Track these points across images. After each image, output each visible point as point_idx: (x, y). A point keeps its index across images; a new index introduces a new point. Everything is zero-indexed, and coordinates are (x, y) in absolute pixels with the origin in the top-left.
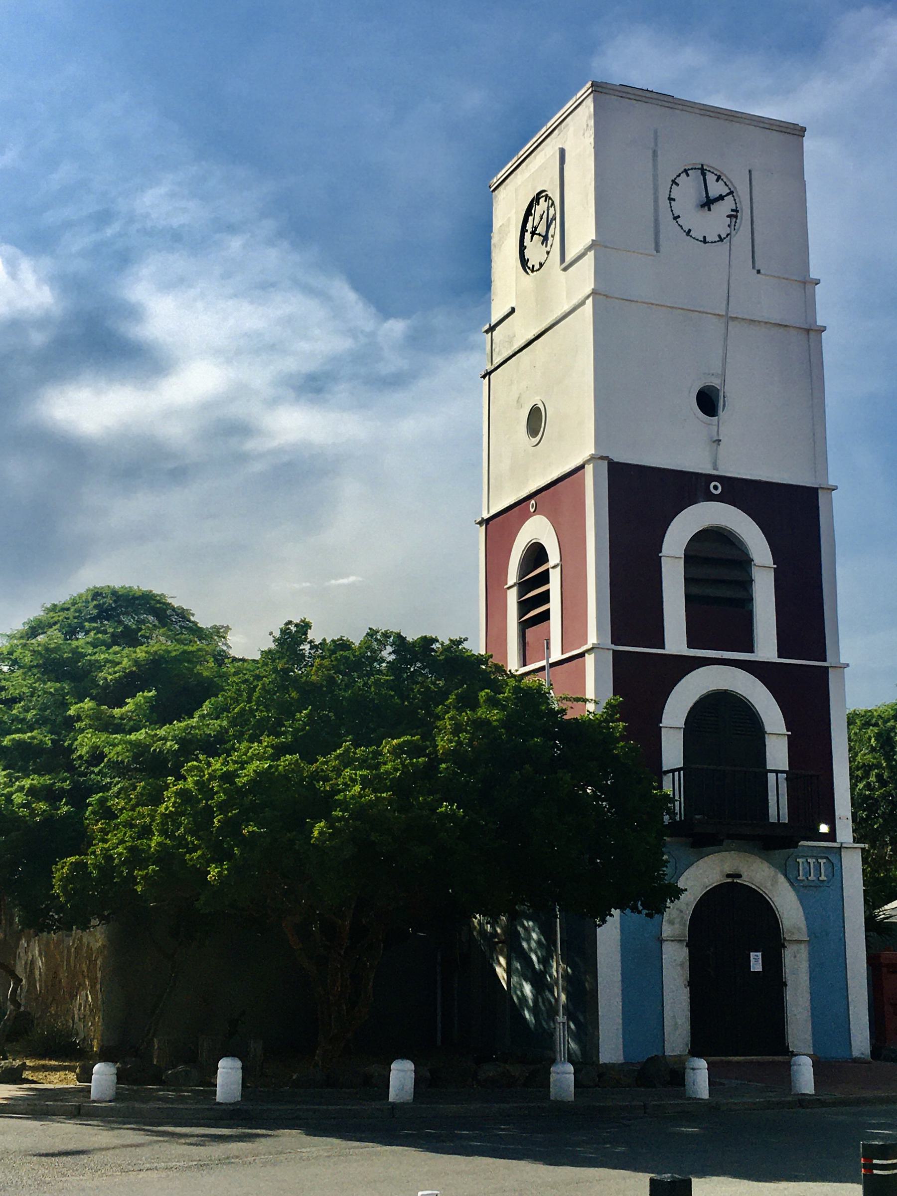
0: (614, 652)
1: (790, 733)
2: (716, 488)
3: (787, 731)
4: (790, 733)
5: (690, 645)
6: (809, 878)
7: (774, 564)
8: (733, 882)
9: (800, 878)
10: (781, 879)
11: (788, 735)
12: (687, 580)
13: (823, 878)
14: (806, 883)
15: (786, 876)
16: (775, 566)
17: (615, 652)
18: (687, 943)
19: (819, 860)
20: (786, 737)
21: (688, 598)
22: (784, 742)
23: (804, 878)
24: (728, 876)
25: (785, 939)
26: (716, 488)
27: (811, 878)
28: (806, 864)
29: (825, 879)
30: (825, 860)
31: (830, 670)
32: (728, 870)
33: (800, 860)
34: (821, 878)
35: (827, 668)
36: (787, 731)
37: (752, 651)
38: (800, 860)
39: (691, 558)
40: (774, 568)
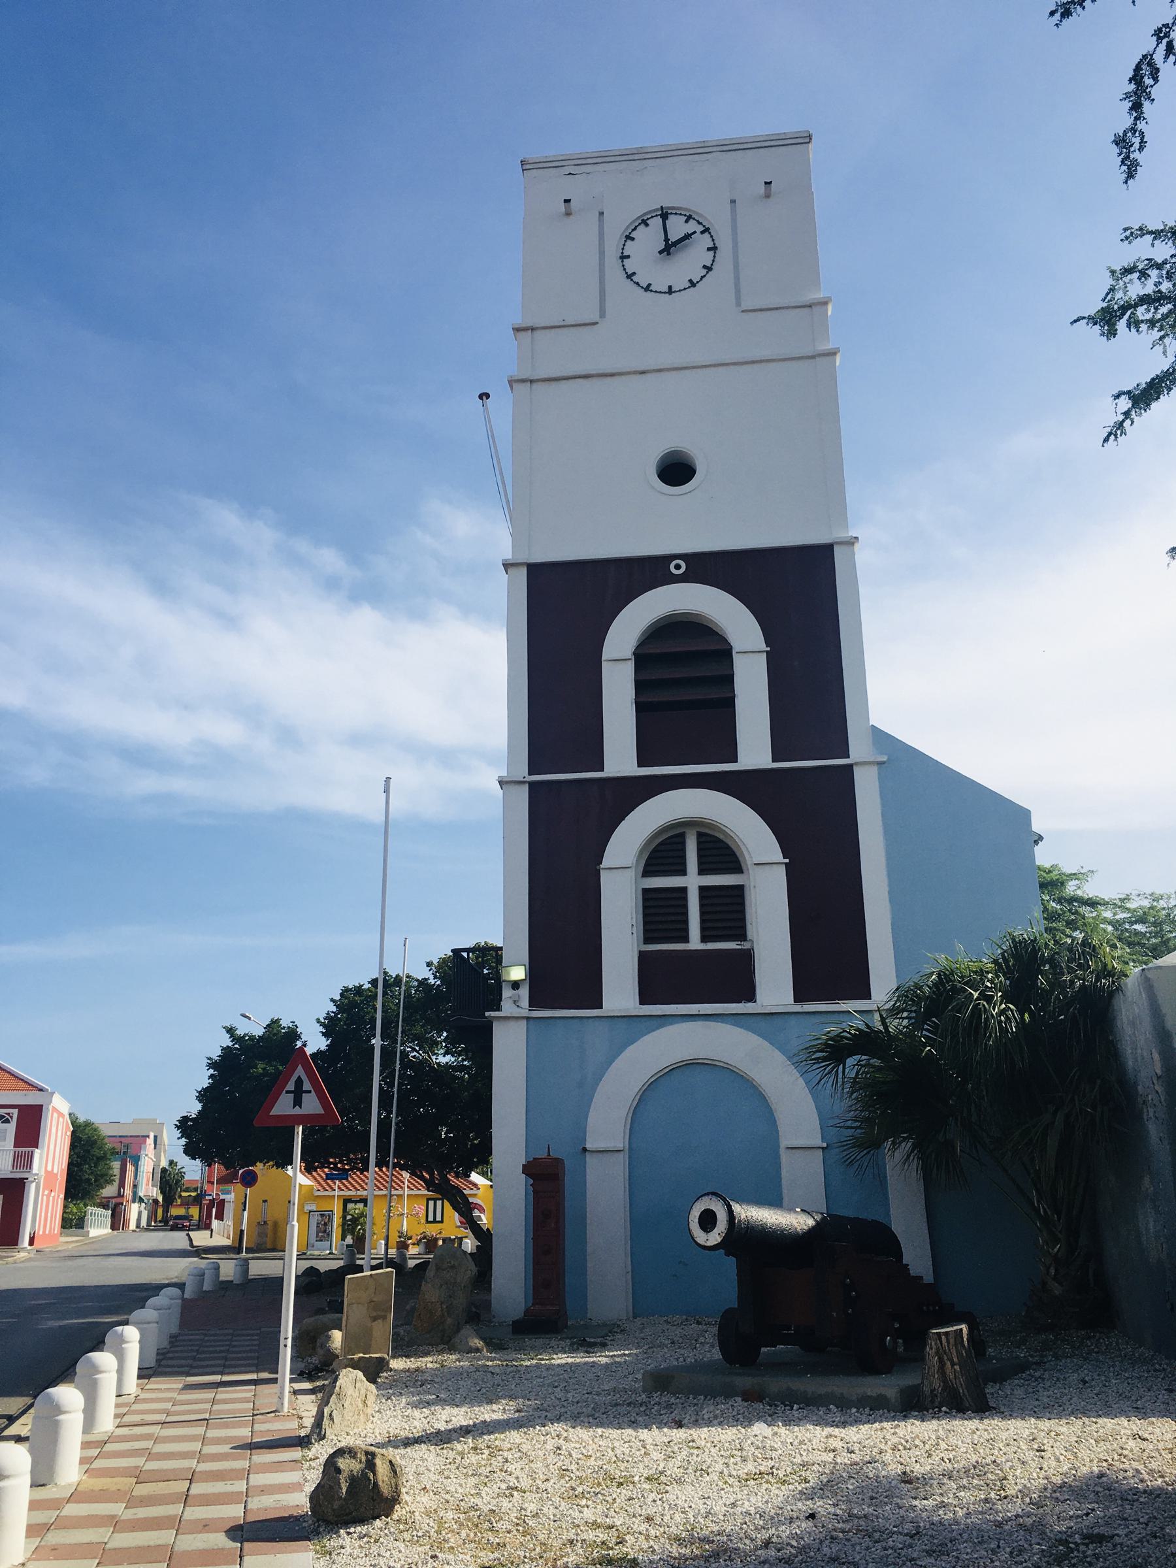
0: (533, 786)
1: (787, 861)
2: (678, 568)
3: (784, 858)
4: (787, 861)
5: (639, 765)
11: (786, 864)
12: (640, 686)
16: (768, 649)
17: (533, 786)
20: (784, 867)
21: (641, 708)
22: (781, 872)
26: (678, 567)
31: (858, 773)
35: (850, 768)
36: (784, 858)
37: (734, 759)
39: (643, 658)
40: (767, 652)
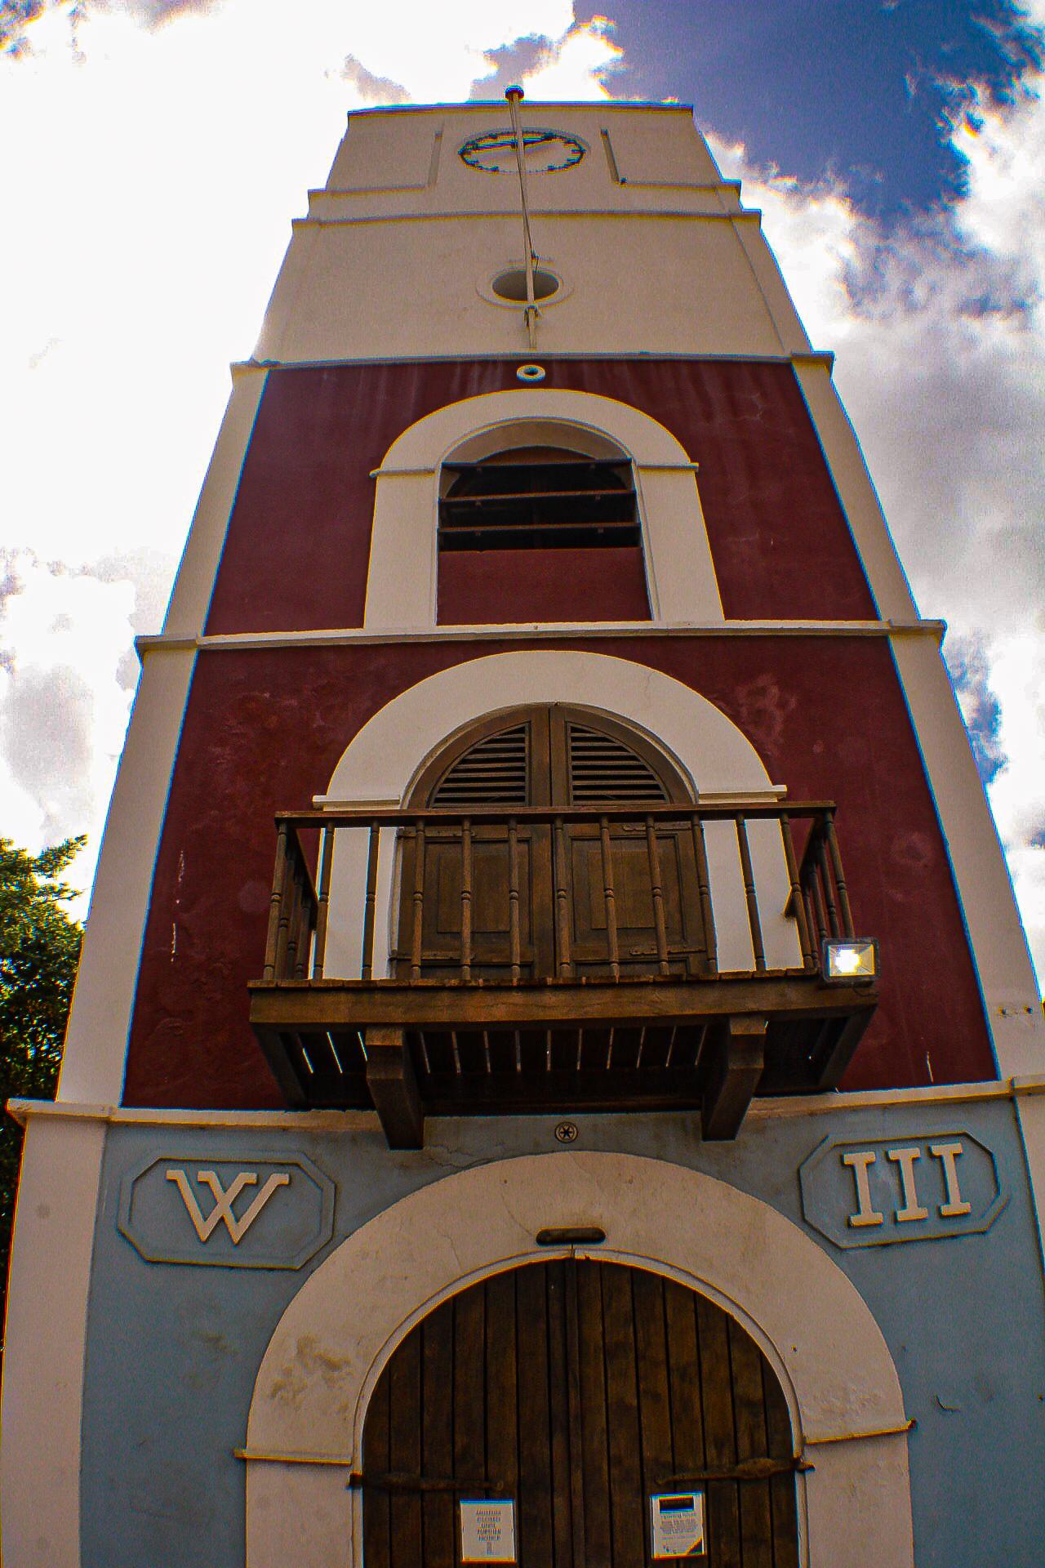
6: (902, 1215)
7: (693, 461)
8: (570, 1261)
9: (866, 1216)
10: (780, 1226)
13: (956, 1206)
14: (889, 1234)
15: (803, 1221)
18: (353, 1477)
19: (936, 1150)
23: (878, 1217)
24: (546, 1239)
25: (803, 1442)
27: (912, 1211)
28: (885, 1174)
29: (965, 1207)
30: (957, 1147)
32: (562, 1215)
33: (858, 1159)
34: (946, 1210)
38: (858, 1159)
